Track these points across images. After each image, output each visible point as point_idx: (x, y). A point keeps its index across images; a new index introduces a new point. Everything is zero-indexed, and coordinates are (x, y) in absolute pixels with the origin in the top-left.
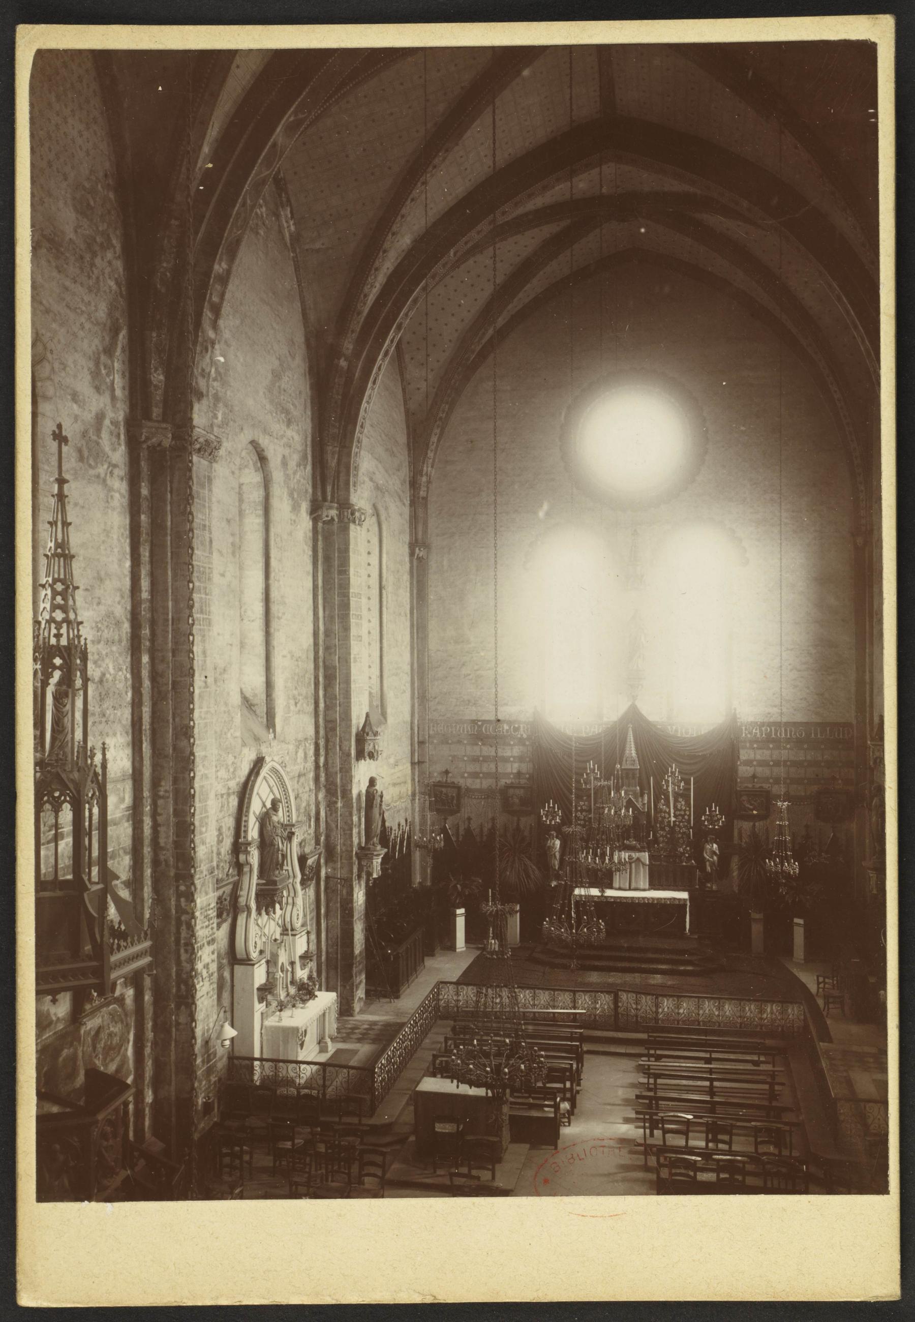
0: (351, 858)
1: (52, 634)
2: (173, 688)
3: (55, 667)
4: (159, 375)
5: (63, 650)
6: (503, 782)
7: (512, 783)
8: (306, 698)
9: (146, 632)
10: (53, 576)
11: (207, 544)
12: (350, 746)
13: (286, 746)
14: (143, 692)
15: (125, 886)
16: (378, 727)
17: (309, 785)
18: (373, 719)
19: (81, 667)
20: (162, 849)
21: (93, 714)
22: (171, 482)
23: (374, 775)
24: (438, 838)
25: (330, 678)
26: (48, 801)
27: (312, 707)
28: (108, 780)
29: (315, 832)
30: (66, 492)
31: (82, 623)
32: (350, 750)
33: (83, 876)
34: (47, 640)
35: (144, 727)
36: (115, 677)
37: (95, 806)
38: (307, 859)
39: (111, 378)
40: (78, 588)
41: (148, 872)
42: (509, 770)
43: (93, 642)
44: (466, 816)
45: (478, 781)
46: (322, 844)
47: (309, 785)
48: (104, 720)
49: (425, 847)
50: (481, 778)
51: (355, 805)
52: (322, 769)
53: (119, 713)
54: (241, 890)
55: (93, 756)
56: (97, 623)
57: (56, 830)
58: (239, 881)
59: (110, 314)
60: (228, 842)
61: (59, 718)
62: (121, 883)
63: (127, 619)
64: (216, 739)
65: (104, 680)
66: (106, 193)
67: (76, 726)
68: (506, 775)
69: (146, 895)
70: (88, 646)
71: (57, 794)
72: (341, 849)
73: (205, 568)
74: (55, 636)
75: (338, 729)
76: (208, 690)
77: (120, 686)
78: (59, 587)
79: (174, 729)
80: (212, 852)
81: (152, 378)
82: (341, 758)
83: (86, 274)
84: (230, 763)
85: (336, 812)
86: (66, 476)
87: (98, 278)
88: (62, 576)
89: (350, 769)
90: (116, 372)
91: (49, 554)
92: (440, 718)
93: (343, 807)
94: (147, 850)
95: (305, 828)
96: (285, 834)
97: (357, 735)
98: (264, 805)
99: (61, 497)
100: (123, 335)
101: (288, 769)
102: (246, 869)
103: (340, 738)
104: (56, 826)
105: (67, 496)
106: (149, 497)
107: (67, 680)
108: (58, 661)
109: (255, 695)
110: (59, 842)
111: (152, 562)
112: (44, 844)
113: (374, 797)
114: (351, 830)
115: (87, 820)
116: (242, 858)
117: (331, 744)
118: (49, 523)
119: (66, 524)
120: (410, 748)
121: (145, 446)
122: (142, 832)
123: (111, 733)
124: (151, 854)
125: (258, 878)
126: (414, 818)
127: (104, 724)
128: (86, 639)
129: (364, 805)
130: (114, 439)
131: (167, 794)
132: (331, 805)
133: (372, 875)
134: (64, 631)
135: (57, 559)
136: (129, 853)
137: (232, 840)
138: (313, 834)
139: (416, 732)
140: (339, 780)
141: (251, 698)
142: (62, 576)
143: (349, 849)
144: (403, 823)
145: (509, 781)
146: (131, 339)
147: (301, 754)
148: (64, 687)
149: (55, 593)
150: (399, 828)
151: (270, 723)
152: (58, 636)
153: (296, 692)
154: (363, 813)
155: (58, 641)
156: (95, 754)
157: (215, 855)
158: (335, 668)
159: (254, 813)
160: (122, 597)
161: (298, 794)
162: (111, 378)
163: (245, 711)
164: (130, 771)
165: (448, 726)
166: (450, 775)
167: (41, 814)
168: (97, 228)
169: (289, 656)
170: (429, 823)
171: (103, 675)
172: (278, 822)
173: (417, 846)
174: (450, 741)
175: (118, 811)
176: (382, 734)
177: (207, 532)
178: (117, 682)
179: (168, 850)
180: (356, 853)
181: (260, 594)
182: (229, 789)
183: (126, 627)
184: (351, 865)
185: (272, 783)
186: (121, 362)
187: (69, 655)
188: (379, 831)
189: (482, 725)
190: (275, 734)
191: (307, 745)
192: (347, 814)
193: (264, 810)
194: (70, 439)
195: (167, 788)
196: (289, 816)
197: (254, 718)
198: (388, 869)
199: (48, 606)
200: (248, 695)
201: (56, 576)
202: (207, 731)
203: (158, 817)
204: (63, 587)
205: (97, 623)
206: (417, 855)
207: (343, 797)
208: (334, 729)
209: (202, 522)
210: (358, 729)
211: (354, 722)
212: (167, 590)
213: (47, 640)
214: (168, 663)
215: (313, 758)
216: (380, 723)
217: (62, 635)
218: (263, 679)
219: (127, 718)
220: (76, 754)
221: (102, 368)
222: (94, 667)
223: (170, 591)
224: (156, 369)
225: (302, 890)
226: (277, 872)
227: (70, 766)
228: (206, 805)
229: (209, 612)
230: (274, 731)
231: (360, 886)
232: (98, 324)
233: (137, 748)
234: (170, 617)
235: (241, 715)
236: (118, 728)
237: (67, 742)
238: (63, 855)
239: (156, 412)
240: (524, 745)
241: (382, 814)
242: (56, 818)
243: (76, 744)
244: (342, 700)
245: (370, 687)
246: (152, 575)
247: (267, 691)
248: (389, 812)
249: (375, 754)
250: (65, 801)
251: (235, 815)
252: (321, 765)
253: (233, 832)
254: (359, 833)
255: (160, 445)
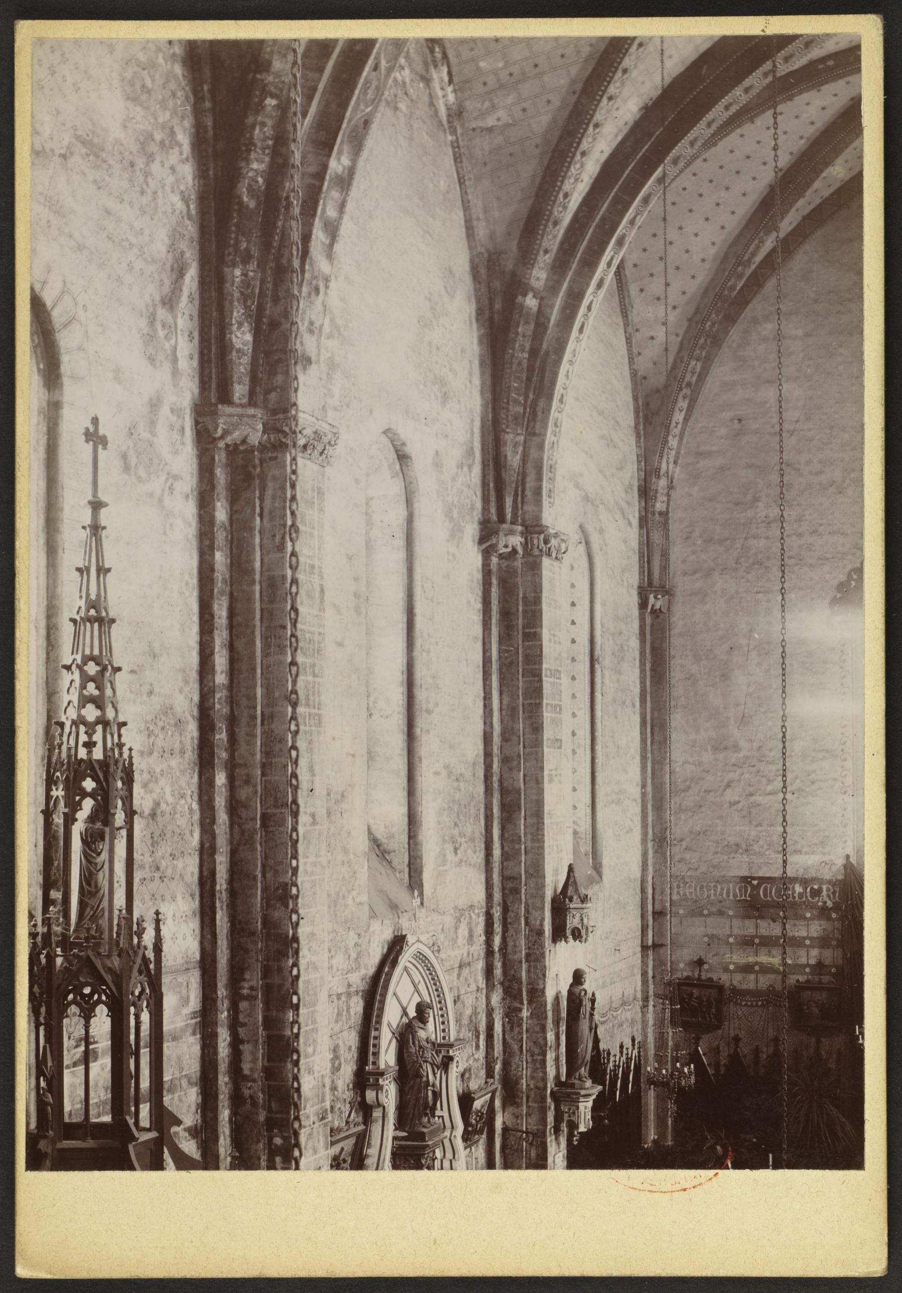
0: (543, 1099)
1: (81, 743)
2: (264, 825)
3: (84, 794)
4: (243, 333)
5: (97, 767)
6: (792, 979)
7: (808, 981)
8: (472, 840)
9: (221, 736)
10: (83, 651)
11: (317, 595)
12: (543, 919)
13: (440, 917)
14: (217, 832)
15: (190, 1134)
16: (586, 888)
17: (476, 981)
18: (583, 872)
19: (123, 793)
20: (246, 1078)
21: (142, 867)
22: (261, 499)
23: (581, 966)
24: (686, 1070)
25: (509, 810)
26: (74, 1002)
27: (481, 855)
28: (163, 970)
29: (486, 1057)
30: (103, 522)
31: (124, 724)
32: (542, 925)
33: (128, 1118)
34: (73, 752)
35: (218, 888)
36: (174, 808)
37: (145, 1009)
38: (473, 1100)
39: (173, 342)
40: (119, 669)
41: (225, 1114)
42: (803, 961)
43: (142, 753)
44: (732, 1034)
45: (752, 977)
46: (497, 1077)
47: (476, 981)
48: (157, 875)
49: (665, 1084)
50: (757, 972)
51: (550, 1014)
52: (497, 955)
53: (180, 864)
54: (369, 1145)
55: (140, 933)
56: (146, 722)
57: (87, 1046)
58: (365, 1131)
59: (172, 248)
60: (348, 1070)
61: (91, 873)
62: (185, 1130)
63: (193, 717)
64: (329, 907)
65: (158, 812)
66: (169, 67)
67: (116, 885)
68: (799, 968)
69: (222, 1151)
70: (134, 760)
71: (87, 990)
72: (528, 1085)
73: (312, 633)
74: (86, 745)
75: (523, 890)
76: (317, 827)
77: (182, 822)
78: (92, 669)
79: (265, 889)
80: (324, 1086)
81: (234, 340)
82: (527, 938)
83: (138, 189)
84: (351, 944)
85: (520, 1025)
86: (103, 496)
87: (155, 193)
88: (96, 652)
89: (543, 955)
90: (179, 331)
91: (78, 618)
92: (689, 874)
93: (532, 1016)
94: (223, 1080)
95: (469, 1049)
96: (439, 1060)
97: (554, 900)
98: (405, 1013)
99: (96, 529)
100: (192, 274)
101: (443, 955)
102: (377, 1114)
103: (527, 905)
104: (87, 1039)
105: (104, 528)
106: (227, 524)
107: (102, 814)
108: (89, 784)
109: (391, 836)
110: (91, 1065)
111: (231, 627)
112: (68, 1067)
113: (581, 1001)
114: (544, 1054)
115: (133, 1031)
116: (370, 1095)
117: (511, 914)
118: (79, 570)
119: (103, 571)
120: (639, 922)
121: (221, 444)
122: (216, 1053)
123: (168, 896)
124: (230, 1086)
125: (396, 1129)
126: (645, 1036)
127: (157, 881)
128: (130, 749)
129: (564, 1014)
130: (176, 436)
131: (254, 993)
132: (511, 1015)
133: (578, 1128)
134: (98, 737)
135: (88, 624)
136: (196, 1084)
137: (355, 1068)
138: (482, 1061)
139: (650, 897)
140: (524, 974)
141: (384, 841)
142: (96, 652)
143: (541, 1085)
144: (628, 1043)
145: (802, 978)
146: (203, 283)
147: (463, 931)
148: (99, 825)
149: (86, 678)
150: (621, 1052)
151: (415, 882)
152: (89, 745)
153: (456, 832)
154: (563, 1028)
155: (90, 752)
156: (144, 929)
157: (327, 1090)
158: (518, 792)
159: (389, 1025)
160: (186, 682)
161: (459, 997)
162: (173, 342)
163: (375, 861)
164: (198, 956)
165: (702, 887)
166: (706, 966)
167: (65, 1021)
168: (156, 119)
169: (444, 773)
170: (670, 1043)
171: (158, 804)
172: (427, 1041)
173: (651, 1082)
174: (705, 912)
175: (179, 1018)
176: (594, 899)
177: (316, 576)
178: (178, 816)
179: (254, 1081)
180: (552, 1091)
181: (399, 674)
182: (349, 985)
183: (192, 729)
184: (543, 1110)
185: (417, 977)
186: (187, 317)
187: (106, 773)
188: (588, 1057)
189: (759, 885)
190: (422, 899)
191: (473, 916)
192: (537, 1029)
193: (405, 1020)
194: (109, 439)
195: (254, 983)
196: (444, 1031)
197: (389, 872)
198: (603, 1118)
199: (74, 697)
200: (379, 836)
201: (87, 652)
202: (314, 894)
203: (240, 1030)
204: (98, 668)
205: (146, 722)
206: (651, 1098)
207: (530, 1002)
208: (517, 891)
209: (309, 561)
210: (555, 891)
211: (549, 879)
212: (254, 670)
213: (73, 752)
214: (255, 786)
215: (484, 938)
216: (591, 881)
217: (95, 744)
218: (404, 810)
219: (192, 873)
220: (115, 929)
221: (159, 326)
222: (142, 791)
223: (259, 671)
224: (240, 325)
225: (465, 1148)
226: (425, 1120)
227: (107, 947)
228: (313, 1012)
229: (319, 704)
230: (421, 894)
231: (558, 1144)
232: (154, 261)
233: (207, 920)
234: (259, 712)
235: (369, 867)
236: (179, 890)
237: (103, 909)
238: (97, 1085)
239: (239, 391)
240: (829, 919)
241: (594, 1029)
242: (87, 1027)
243: (116, 913)
244: (529, 844)
245: (574, 822)
246: (231, 647)
247: (409, 830)
248: (605, 1026)
249: (583, 932)
250: (99, 1001)
251: (358, 1028)
252: (496, 949)
253: (356, 1055)
254: (557, 1059)
255: (244, 442)
